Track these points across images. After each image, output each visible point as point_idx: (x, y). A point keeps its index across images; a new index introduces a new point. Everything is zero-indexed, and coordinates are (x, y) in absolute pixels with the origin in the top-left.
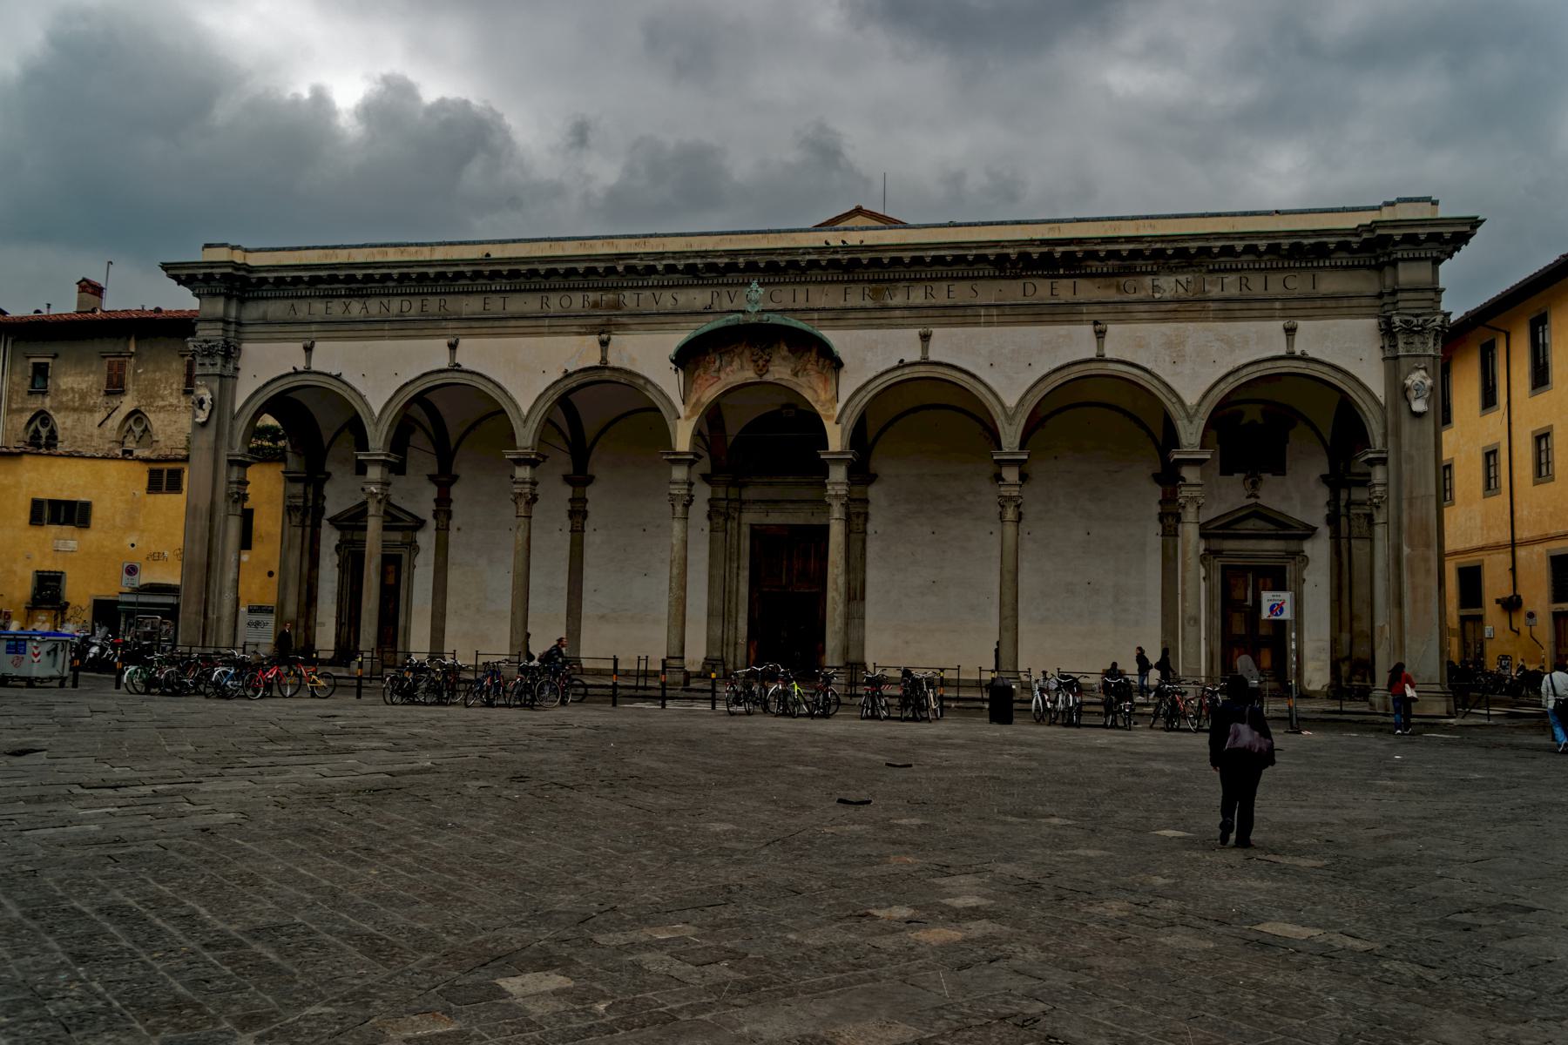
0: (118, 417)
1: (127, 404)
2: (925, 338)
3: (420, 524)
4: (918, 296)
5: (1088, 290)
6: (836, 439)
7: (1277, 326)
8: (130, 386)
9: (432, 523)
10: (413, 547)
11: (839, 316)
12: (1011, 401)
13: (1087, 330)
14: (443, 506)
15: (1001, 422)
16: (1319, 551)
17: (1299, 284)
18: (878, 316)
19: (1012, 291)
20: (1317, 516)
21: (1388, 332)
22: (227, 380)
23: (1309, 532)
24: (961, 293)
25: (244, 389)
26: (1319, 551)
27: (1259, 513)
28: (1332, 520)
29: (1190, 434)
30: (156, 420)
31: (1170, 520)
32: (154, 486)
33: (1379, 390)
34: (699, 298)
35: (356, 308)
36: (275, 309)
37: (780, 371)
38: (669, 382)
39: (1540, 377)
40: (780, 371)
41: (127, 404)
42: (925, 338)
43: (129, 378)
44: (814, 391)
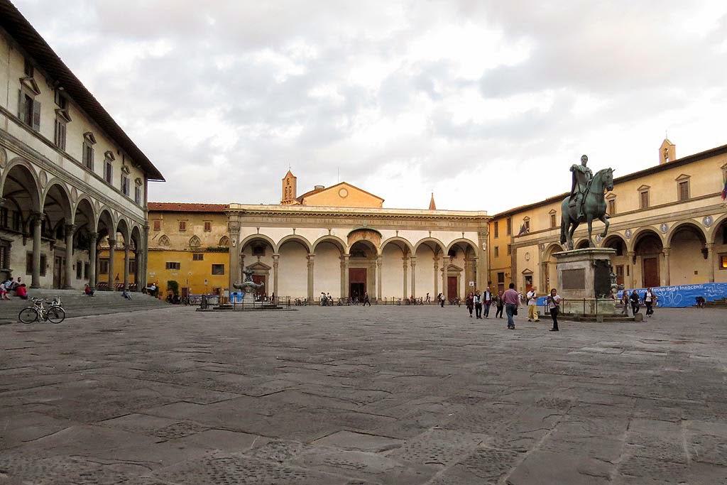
0: (158, 237)
1: (162, 233)
2: (397, 232)
3: (270, 268)
4: (395, 224)
5: (428, 224)
6: (379, 252)
7: (461, 233)
8: (161, 228)
9: (273, 268)
10: (268, 273)
11: (381, 227)
12: (414, 245)
13: (428, 232)
14: (276, 265)
15: (411, 249)
16: (463, 273)
17: (465, 225)
18: (388, 227)
19: (414, 223)
20: (463, 267)
21: (479, 234)
22: (238, 235)
23: (462, 270)
24: (404, 223)
25: (242, 238)
26: (463, 273)
27: (452, 266)
28: (465, 267)
29: (446, 252)
30: (171, 238)
31: (436, 267)
32: (195, 258)
33: (478, 245)
34: (350, 221)
35: (270, 219)
36: (249, 219)
37: (368, 237)
38: (345, 240)
39: (496, 235)
40: (368, 237)
41: (162, 233)
42: (397, 232)
43: (161, 225)
44: (375, 241)
